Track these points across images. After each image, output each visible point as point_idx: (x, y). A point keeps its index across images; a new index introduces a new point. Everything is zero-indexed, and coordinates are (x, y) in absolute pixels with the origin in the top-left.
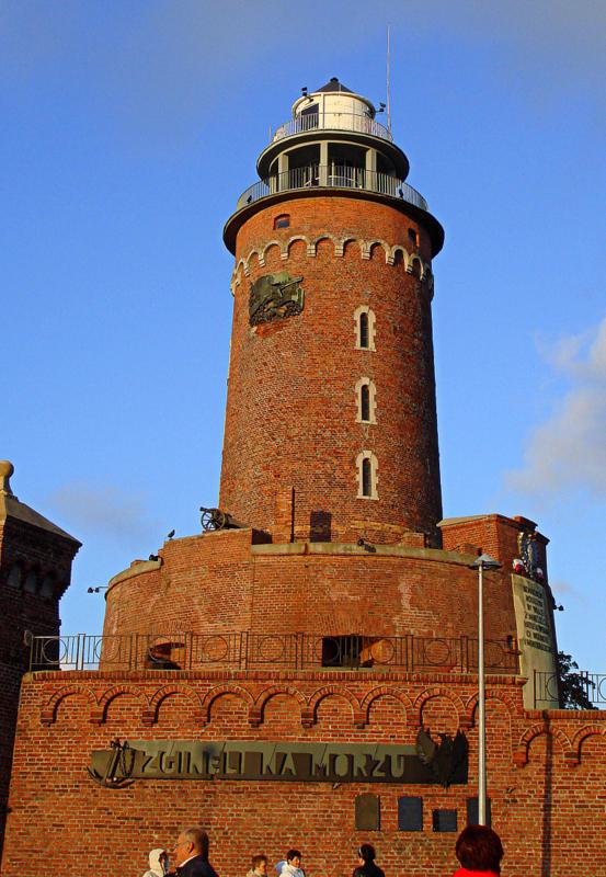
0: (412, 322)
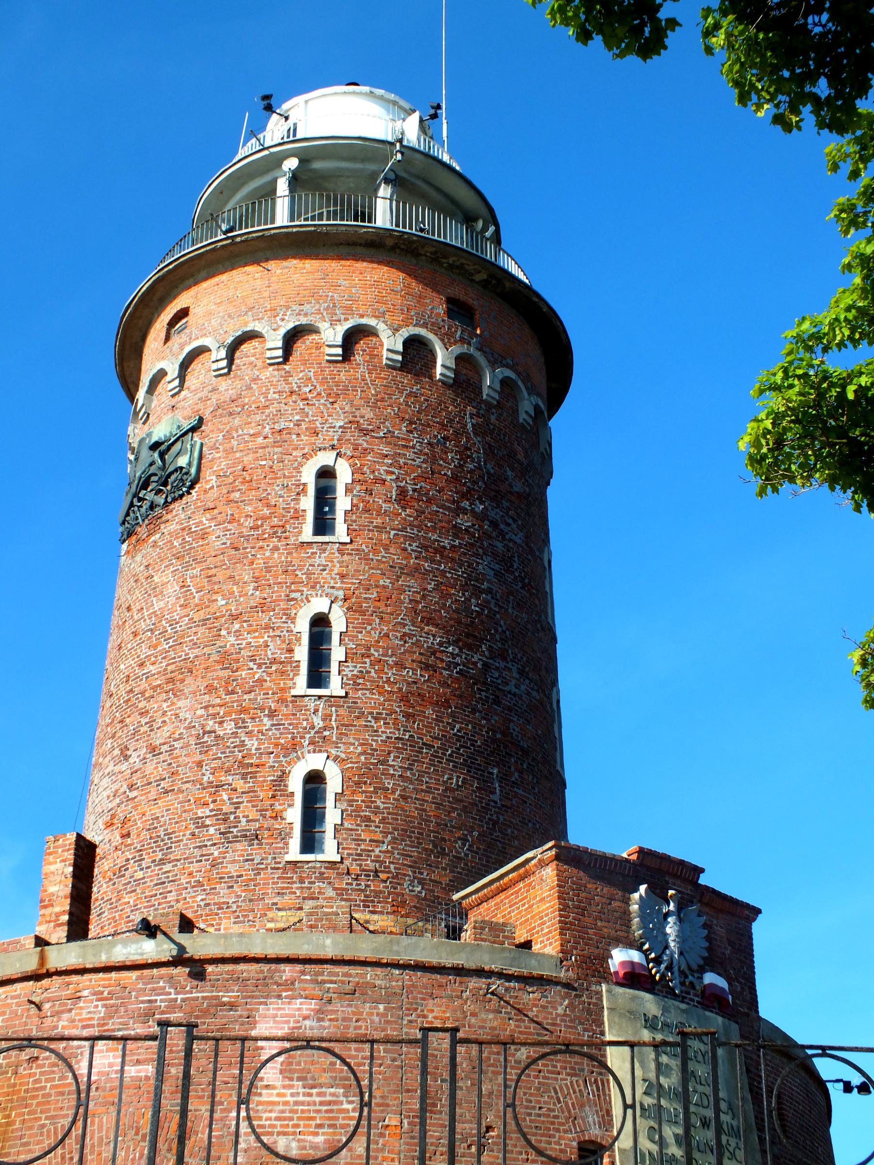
0: (455, 478)
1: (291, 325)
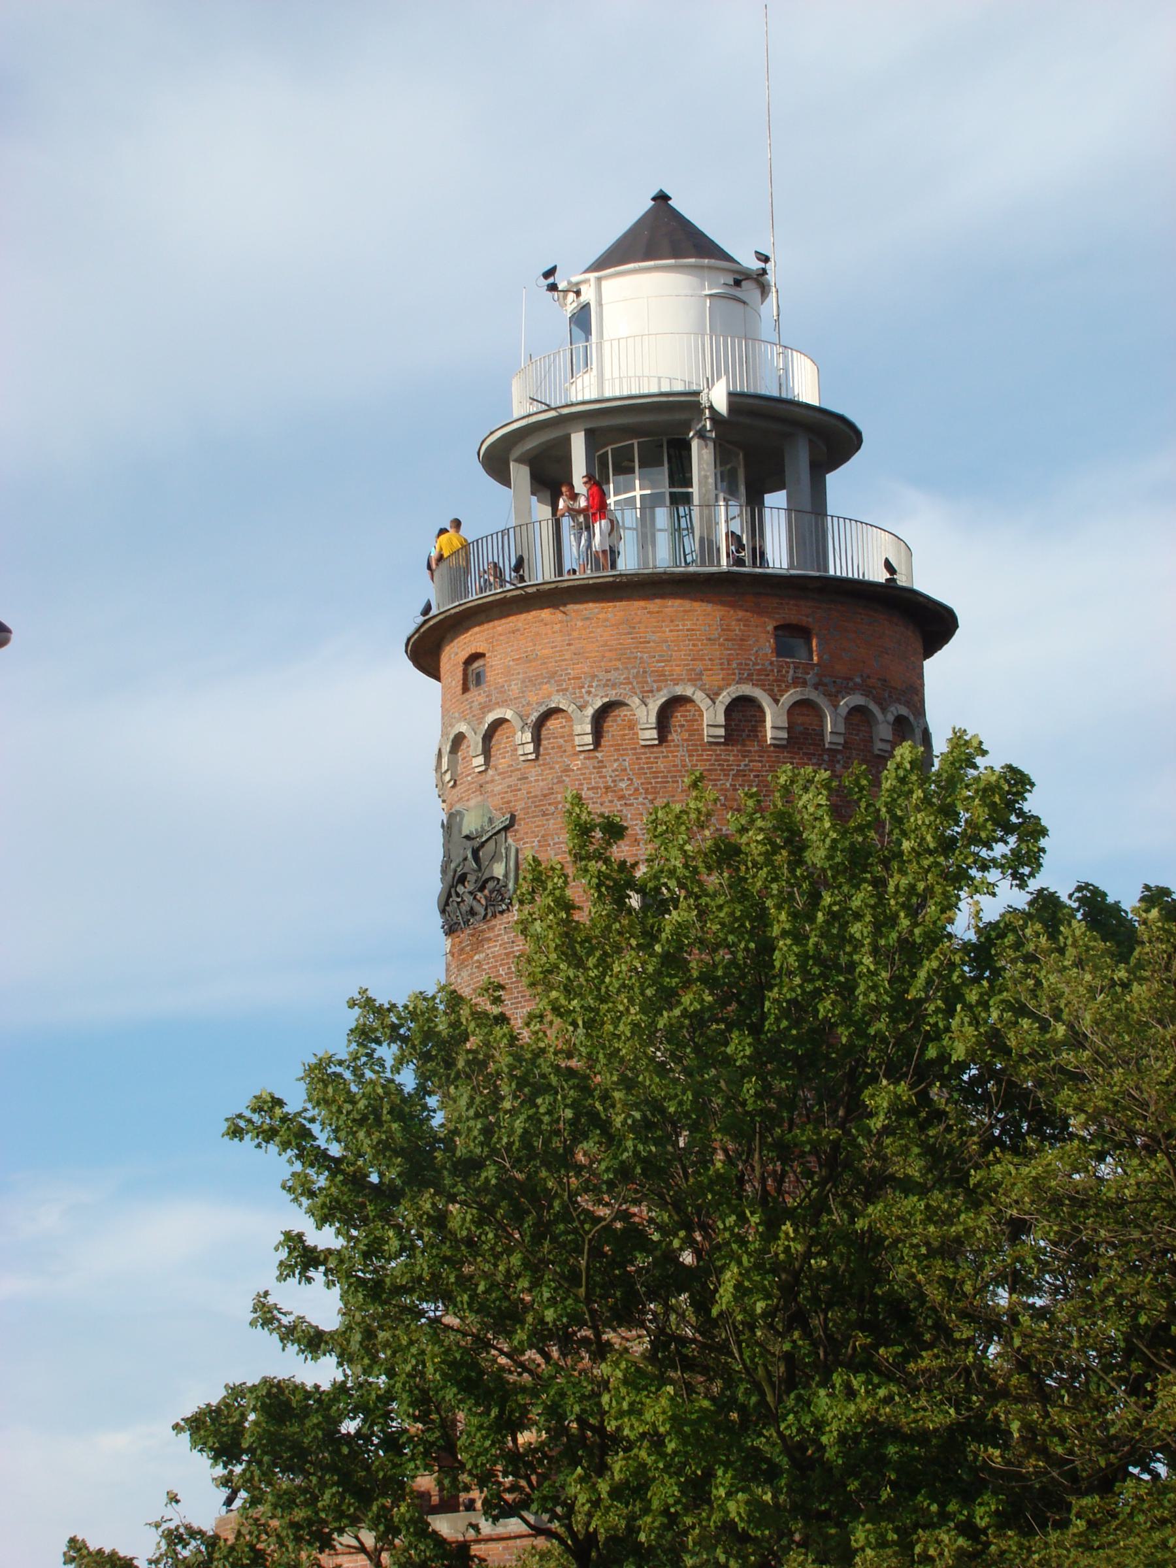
1: (598, 703)
